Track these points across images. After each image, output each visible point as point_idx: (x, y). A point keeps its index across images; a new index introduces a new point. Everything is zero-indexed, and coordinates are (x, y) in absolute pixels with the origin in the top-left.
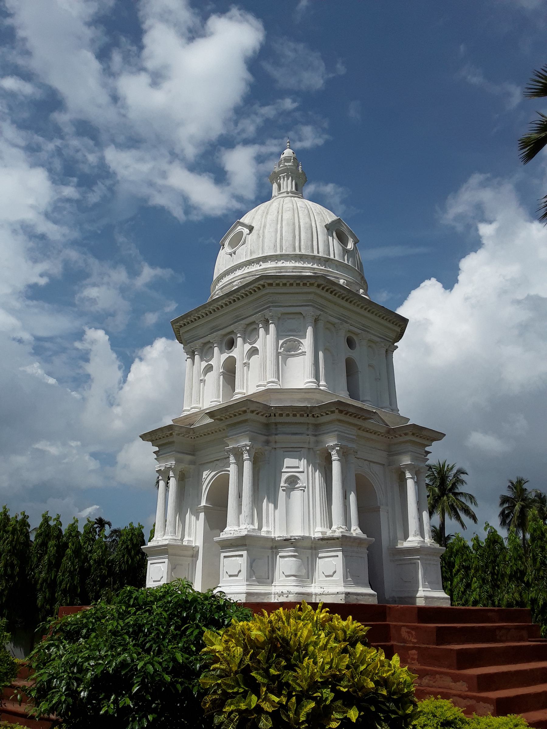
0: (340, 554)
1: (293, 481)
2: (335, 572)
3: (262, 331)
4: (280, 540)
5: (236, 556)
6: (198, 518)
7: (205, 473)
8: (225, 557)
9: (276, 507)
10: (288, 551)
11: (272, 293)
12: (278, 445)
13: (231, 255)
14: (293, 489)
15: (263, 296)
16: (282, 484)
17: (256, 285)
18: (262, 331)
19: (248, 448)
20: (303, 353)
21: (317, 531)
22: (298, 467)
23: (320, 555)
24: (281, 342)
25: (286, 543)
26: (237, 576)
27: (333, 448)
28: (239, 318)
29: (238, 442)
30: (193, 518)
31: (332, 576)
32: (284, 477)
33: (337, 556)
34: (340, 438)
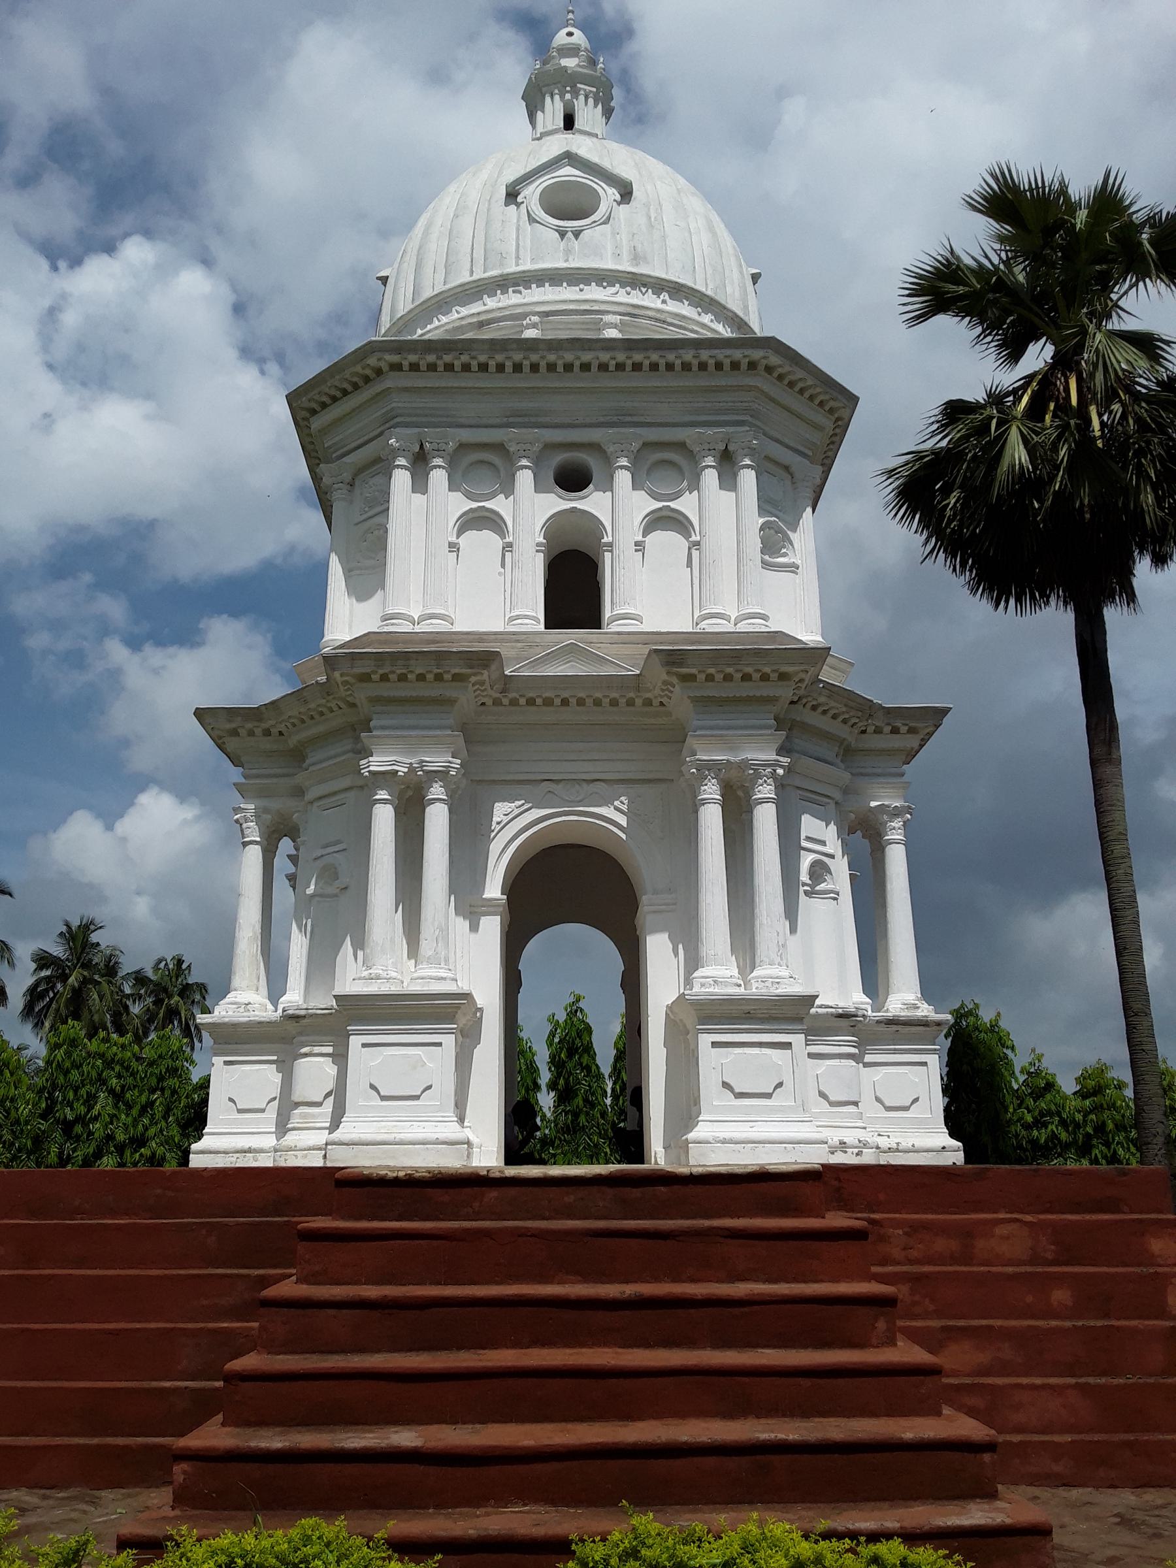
2: (916, 1100)
3: (710, 477)
4: (827, 1013)
5: (761, 1045)
6: (474, 928)
7: (501, 810)
8: (715, 1044)
13: (562, 234)
17: (737, 354)
18: (710, 477)
19: (780, 771)
20: (793, 568)
22: (823, 843)
25: (844, 1023)
26: (768, 1096)
27: (896, 813)
28: (629, 419)
29: (733, 749)
30: (462, 924)
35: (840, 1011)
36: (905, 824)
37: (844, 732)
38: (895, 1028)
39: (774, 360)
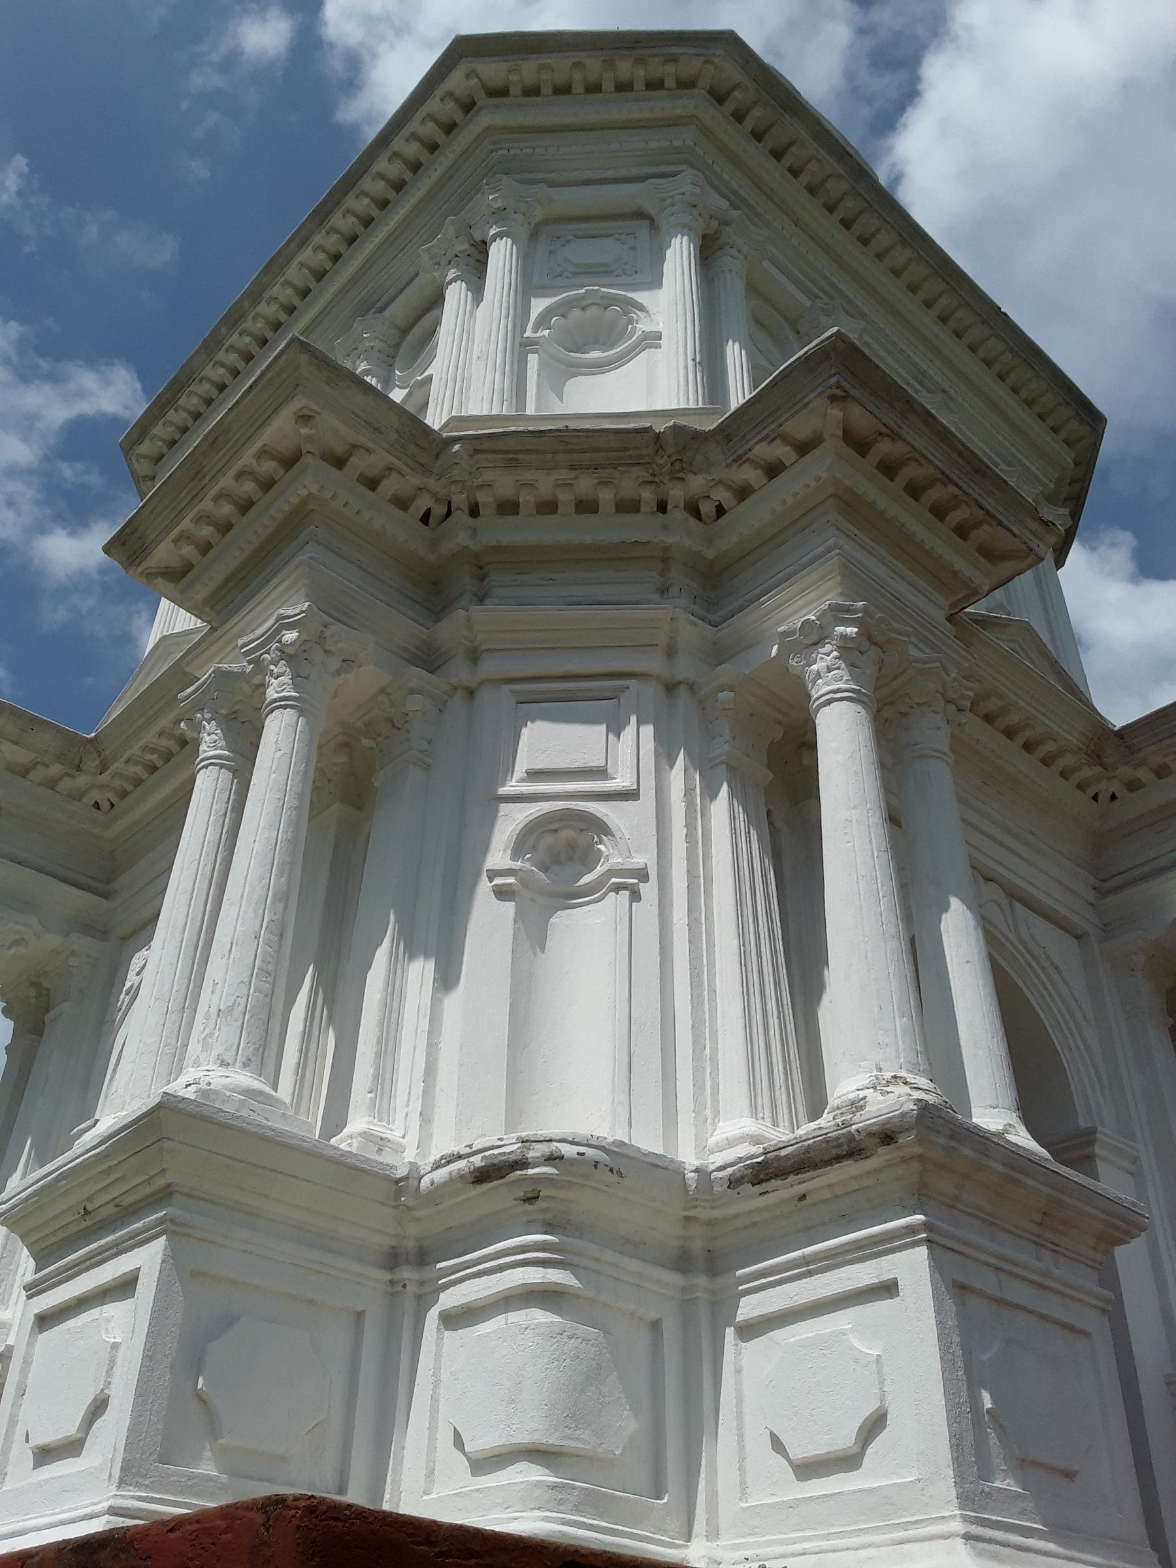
0: (912, 1266)
1: (566, 853)
2: (875, 1425)
4: (451, 1181)
9: (447, 979)
10: (510, 1264)
11: (510, 130)
12: (490, 667)
14: (569, 897)
15: (465, 154)
16: (498, 857)
21: (726, 1126)
22: (601, 773)
23: (749, 1308)
24: (539, 305)
25: (498, 1196)
27: (814, 636)
31: (848, 1461)
32: (511, 821)
33: (888, 1289)
34: (854, 579)
35: (477, 1160)
36: (847, 649)
37: (641, 528)
38: (784, 1190)
39: (493, 70)
